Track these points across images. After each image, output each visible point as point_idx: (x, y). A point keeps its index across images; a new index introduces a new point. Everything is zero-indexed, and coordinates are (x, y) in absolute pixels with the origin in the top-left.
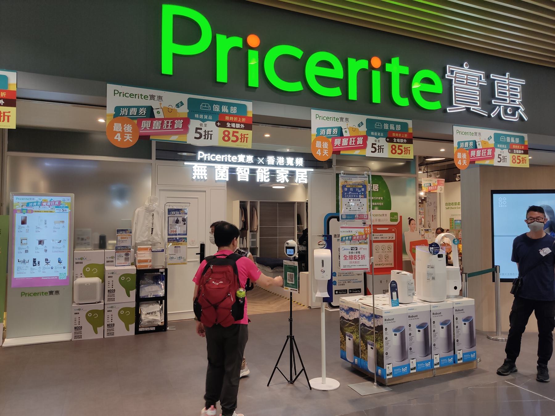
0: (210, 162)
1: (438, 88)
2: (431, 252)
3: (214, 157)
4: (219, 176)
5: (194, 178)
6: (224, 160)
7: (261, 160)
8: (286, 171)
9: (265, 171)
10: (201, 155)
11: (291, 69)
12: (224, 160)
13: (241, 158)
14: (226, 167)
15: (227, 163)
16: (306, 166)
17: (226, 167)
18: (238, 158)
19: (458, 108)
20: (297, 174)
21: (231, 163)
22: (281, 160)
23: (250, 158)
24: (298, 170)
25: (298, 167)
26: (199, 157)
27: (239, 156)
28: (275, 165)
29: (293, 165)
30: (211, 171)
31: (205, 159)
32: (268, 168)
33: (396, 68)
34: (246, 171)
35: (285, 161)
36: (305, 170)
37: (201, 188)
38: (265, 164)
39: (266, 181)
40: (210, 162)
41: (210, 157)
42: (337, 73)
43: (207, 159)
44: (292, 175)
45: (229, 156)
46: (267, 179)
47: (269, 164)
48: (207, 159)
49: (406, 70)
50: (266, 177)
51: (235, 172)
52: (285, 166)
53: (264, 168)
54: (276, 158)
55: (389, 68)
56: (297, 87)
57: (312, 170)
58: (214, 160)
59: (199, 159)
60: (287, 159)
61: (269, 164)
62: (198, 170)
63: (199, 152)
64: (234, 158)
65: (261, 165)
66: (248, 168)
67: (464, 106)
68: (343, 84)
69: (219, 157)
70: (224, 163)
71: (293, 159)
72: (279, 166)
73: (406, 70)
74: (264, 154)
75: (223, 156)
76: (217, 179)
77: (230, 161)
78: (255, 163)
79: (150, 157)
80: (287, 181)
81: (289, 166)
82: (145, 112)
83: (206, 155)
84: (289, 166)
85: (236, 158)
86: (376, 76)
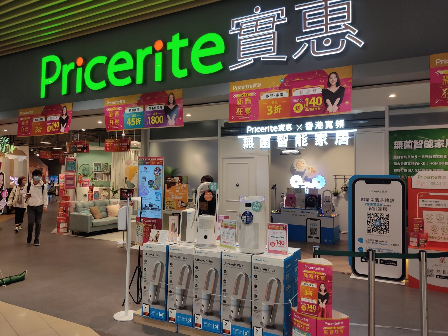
0: (257, 134)
1: (220, 48)
2: (243, 221)
3: (259, 130)
4: (263, 145)
5: (244, 148)
6: (267, 131)
7: (299, 127)
8: (325, 134)
9: (303, 136)
10: (249, 129)
11: (99, 73)
12: (267, 131)
13: (281, 127)
14: (269, 136)
15: (270, 133)
16: (347, 127)
17: (269, 136)
18: (278, 128)
19: (245, 61)
20: (337, 136)
21: (274, 133)
22: (319, 125)
23: (289, 127)
24: (337, 132)
25: (339, 129)
26: (248, 131)
27: (279, 126)
28: (314, 130)
29: (332, 127)
30: (256, 141)
31: (252, 132)
32: (306, 134)
33: (176, 44)
34: (286, 138)
35: (324, 124)
36: (347, 132)
37: (250, 155)
38: (304, 130)
39: (304, 145)
40: (257, 134)
41: (256, 129)
42: (129, 66)
43: (254, 132)
44: (331, 138)
45: (271, 127)
46: (305, 143)
47: (307, 129)
48: (254, 132)
49: (185, 43)
50: (303, 142)
51: (276, 139)
52: (324, 129)
53: (302, 133)
54: (314, 123)
55: (170, 46)
56: (102, 85)
57: (355, 130)
58: (259, 132)
59: (248, 133)
60: (326, 122)
61: (307, 129)
62: (247, 141)
63: (248, 127)
64: (275, 128)
65: (300, 131)
66: (287, 135)
67: (252, 58)
68: (132, 73)
69: (263, 129)
70: (267, 133)
71: (332, 122)
72: (318, 130)
73: (185, 43)
74: (302, 122)
75: (266, 128)
76: (261, 147)
77: (272, 131)
78: (294, 130)
79: (217, 136)
80: (327, 144)
81: (329, 129)
82: (250, 101)
83: (253, 128)
84: (329, 129)
85: (277, 128)
86: (159, 57)
